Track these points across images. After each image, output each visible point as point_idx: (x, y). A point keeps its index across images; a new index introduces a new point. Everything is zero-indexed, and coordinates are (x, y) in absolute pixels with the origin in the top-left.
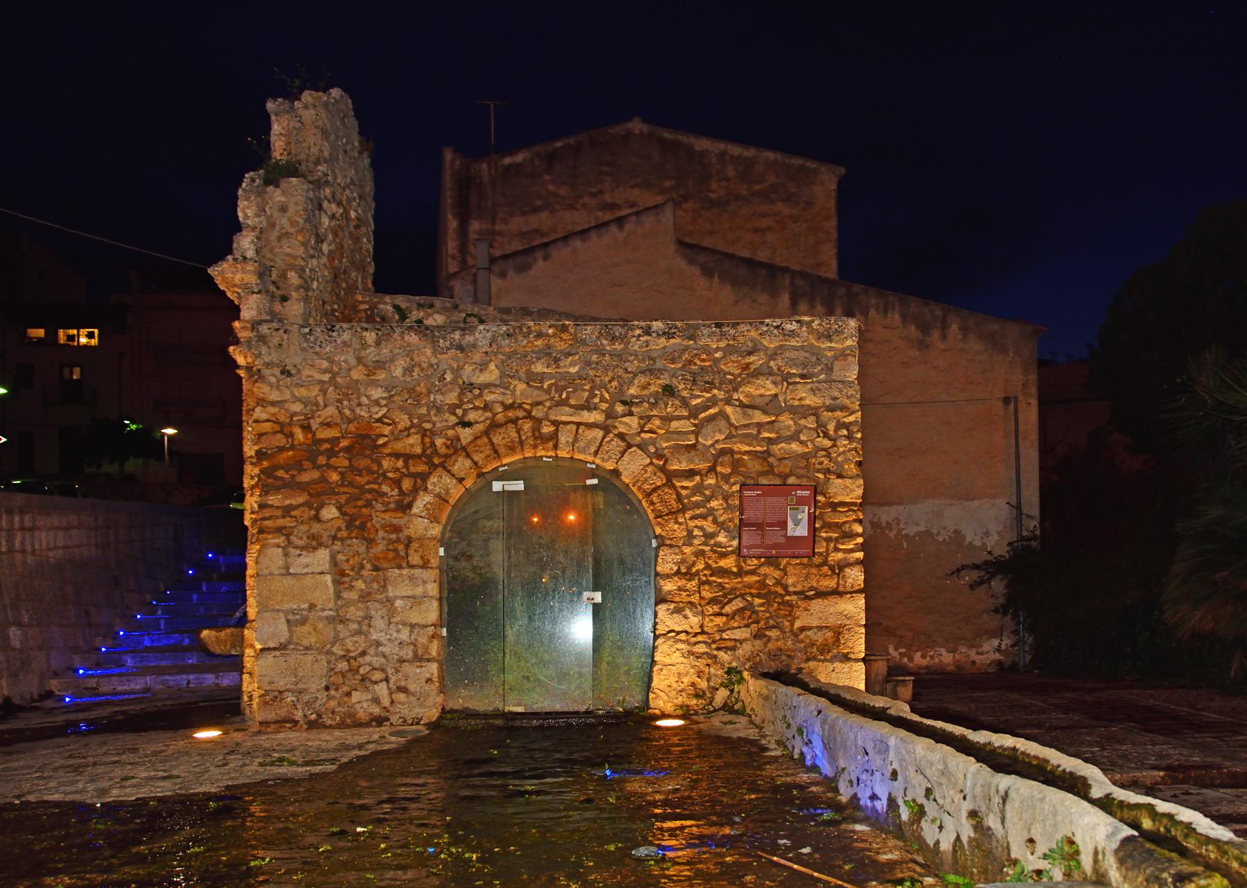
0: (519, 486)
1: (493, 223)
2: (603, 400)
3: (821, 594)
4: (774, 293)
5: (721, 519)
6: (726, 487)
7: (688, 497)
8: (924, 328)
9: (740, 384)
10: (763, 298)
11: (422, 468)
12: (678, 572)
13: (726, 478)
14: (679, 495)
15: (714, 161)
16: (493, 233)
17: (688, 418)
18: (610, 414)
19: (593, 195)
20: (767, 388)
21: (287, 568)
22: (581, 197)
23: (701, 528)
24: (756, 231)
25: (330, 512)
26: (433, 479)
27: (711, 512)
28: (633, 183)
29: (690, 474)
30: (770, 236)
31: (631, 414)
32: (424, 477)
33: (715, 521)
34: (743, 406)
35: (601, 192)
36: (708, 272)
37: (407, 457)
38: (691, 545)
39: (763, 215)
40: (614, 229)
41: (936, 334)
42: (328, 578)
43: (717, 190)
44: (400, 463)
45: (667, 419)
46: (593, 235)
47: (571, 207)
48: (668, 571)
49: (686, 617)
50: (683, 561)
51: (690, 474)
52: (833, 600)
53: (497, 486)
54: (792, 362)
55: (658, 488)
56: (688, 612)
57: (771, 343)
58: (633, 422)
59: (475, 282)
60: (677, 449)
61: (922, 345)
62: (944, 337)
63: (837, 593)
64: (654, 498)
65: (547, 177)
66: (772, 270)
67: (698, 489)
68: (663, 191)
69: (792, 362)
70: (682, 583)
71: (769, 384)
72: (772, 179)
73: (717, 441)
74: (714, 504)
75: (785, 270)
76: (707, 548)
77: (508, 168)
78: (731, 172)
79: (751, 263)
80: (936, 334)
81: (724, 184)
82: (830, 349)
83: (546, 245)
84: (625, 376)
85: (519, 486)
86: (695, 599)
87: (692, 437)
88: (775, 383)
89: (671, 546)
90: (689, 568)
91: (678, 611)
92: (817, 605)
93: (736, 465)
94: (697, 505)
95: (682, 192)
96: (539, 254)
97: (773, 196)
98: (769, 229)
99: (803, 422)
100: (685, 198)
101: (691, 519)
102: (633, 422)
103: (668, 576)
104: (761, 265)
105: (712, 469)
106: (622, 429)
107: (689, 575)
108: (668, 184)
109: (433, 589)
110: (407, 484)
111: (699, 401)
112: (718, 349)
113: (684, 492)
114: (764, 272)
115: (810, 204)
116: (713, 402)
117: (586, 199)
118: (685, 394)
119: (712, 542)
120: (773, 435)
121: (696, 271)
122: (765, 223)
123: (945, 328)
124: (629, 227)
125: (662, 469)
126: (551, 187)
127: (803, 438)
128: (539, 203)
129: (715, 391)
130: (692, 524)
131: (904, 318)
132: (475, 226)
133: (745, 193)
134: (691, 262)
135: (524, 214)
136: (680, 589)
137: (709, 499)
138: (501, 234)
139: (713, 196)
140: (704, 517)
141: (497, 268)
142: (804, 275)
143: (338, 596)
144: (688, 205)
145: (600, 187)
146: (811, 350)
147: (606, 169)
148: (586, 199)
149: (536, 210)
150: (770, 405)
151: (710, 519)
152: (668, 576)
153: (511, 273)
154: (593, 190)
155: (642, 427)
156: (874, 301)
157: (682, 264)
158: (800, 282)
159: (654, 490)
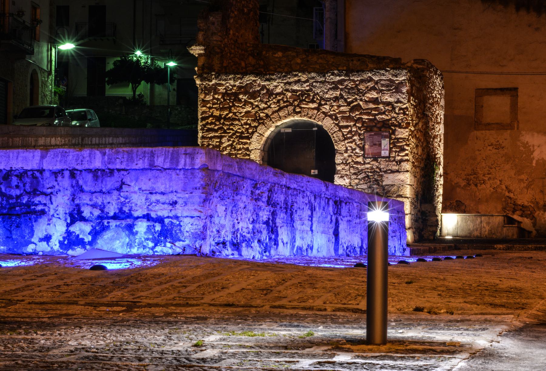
2: (317, 99)
3: (393, 172)
5: (358, 143)
6: (360, 132)
7: (346, 135)
9: (366, 93)
12: (342, 163)
13: (360, 128)
14: (343, 134)
17: (346, 106)
18: (320, 105)
20: (374, 95)
23: (351, 147)
26: (259, 128)
27: (354, 140)
29: (347, 127)
31: (327, 104)
33: (356, 144)
34: (366, 101)
38: (347, 153)
45: (339, 106)
48: (339, 162)
49: (344, 179)
50: (344, 159)
51: (347, 127)
52: (396, 174)
54: (383, 85)
55: (336, 132)
56: (345, 178)
57: (376, 78)
58: (327, 107)
60: (343, 118)
64: (334, 135)
67: (350, 132)
69: (383, 85)
70: (343, 166)
71: (375, 93)
73: (357, 115)
74: (355, 138)
76: (353, 154)
82: (397, 80)
84: (325, 91)
86: (348, 173)
87: (348, 113)
88: (377, 93)
89: (340, 153)
90: (346, 162)
91: (342, 177)
92: (391, 176)
93: (363, 123)
94: (351, 138)
99: (387, 108)
101: (348, 143)
102: (327, 107)
103: (339, 164)
105: (355, 125)
106: (324, 110)
107: (346, 164)
111: (351, 100)
112: (357, 80)
113: (345, 133)
116: (356, 100)
118: (346, 97)
119: (354, 152)
120: (376, 113)
125: (337, 125)
127: (387, 113)
129: (356, 96)
130: (347, 145)
136: (343, 169)
137: (353, 136)
140: (351, 142)
146: (390, 80)
150: (375, 101)
151: (354, 143)
152: (339, 164)
155: (330, 109)
159: (334, 133)
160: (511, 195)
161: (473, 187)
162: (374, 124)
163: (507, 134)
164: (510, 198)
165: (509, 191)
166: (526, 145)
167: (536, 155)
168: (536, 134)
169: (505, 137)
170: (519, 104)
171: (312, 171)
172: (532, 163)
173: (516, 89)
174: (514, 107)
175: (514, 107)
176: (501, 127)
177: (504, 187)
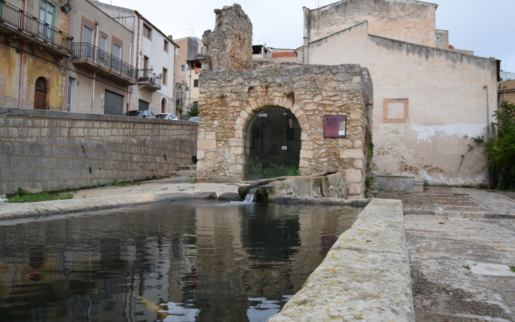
0: (265, 115)
1: (318, 30)
4: (401, 51)
8: (454, 61)
10: (397, 52)
11: (239, 110)
15: (392, 5)
16: (318, 33)
19: (351, 19)
21: (205, 137)
22: (347, 20)
24: (407, 28)
25: (216, 122)
28: (365, 14)
30: (411, 30)
32: (239, 112)
35: (354, 18)
36: (378, 44)
37: (235, 107)
39: (409, 23)
40: (347, 31)
41: (458, 63)
42: (215, 140)
43: (393, 14)
44: (234, 109)
46: (341, 34)
47: (344, 23)
53: (260, 115)
59: (303, 51)
61: (453, 67)
62: (461, 64)
63: (353, 148)
65: (336, 14)
66: (400, 43)
68: (375, 16)
72: (412, 10)
75: (404, 43)
77: (323, 12)
78: (398, 8)
79: (393, 41)
80: (458, 63)
81: (396, 12)
83: (326, 38)
85: (265, 115)
95: (381, 16)
96: (324, 41)
97: (412, 16)
98: (412, 27)
100: (382, 18)
104: (396, 41)
108: (376, 13)
109: (241, 144)
110: (235, 114)
114: (397, 43)
115: (426, 18)
117: (349, 20)
121: (375, 44)
122: (409, 25)
123: (461, 60)
124: (353, 30)
126: (337, 17)
128: (333, 22)
131: (447, 58)
132: (312, 31)
133: (403, 15)
134: (373, 41)
135: (328, 26)
138: (321, 33)
139: (392, 17)
141: (311, 46)
142: (411, 44)
143: (217, 145)
144: (384, 20)
145: (353, 16)
147: (355, 10)
148: (349, 20)
149: (332, 25)
153: (315, 47)
154: (351, 17)
156: (436, 52)
157: (370, 42)
158: (409, 46)
160: (404, 161)
161: (381, 155)
162: (333, 109)
163: (402, 125)
164: (403, 162)
165: (403, 159)
166: (413, 132)
167: (420, 137)
168: (419, 125)
169: (401, 127)
170: (410, 108)
171: (283, 147)
172: (416, 142)
173: (407, 99)
174: (406, 109)
175: (406, 109)
176: (399, 121)
177: (400, 156)
